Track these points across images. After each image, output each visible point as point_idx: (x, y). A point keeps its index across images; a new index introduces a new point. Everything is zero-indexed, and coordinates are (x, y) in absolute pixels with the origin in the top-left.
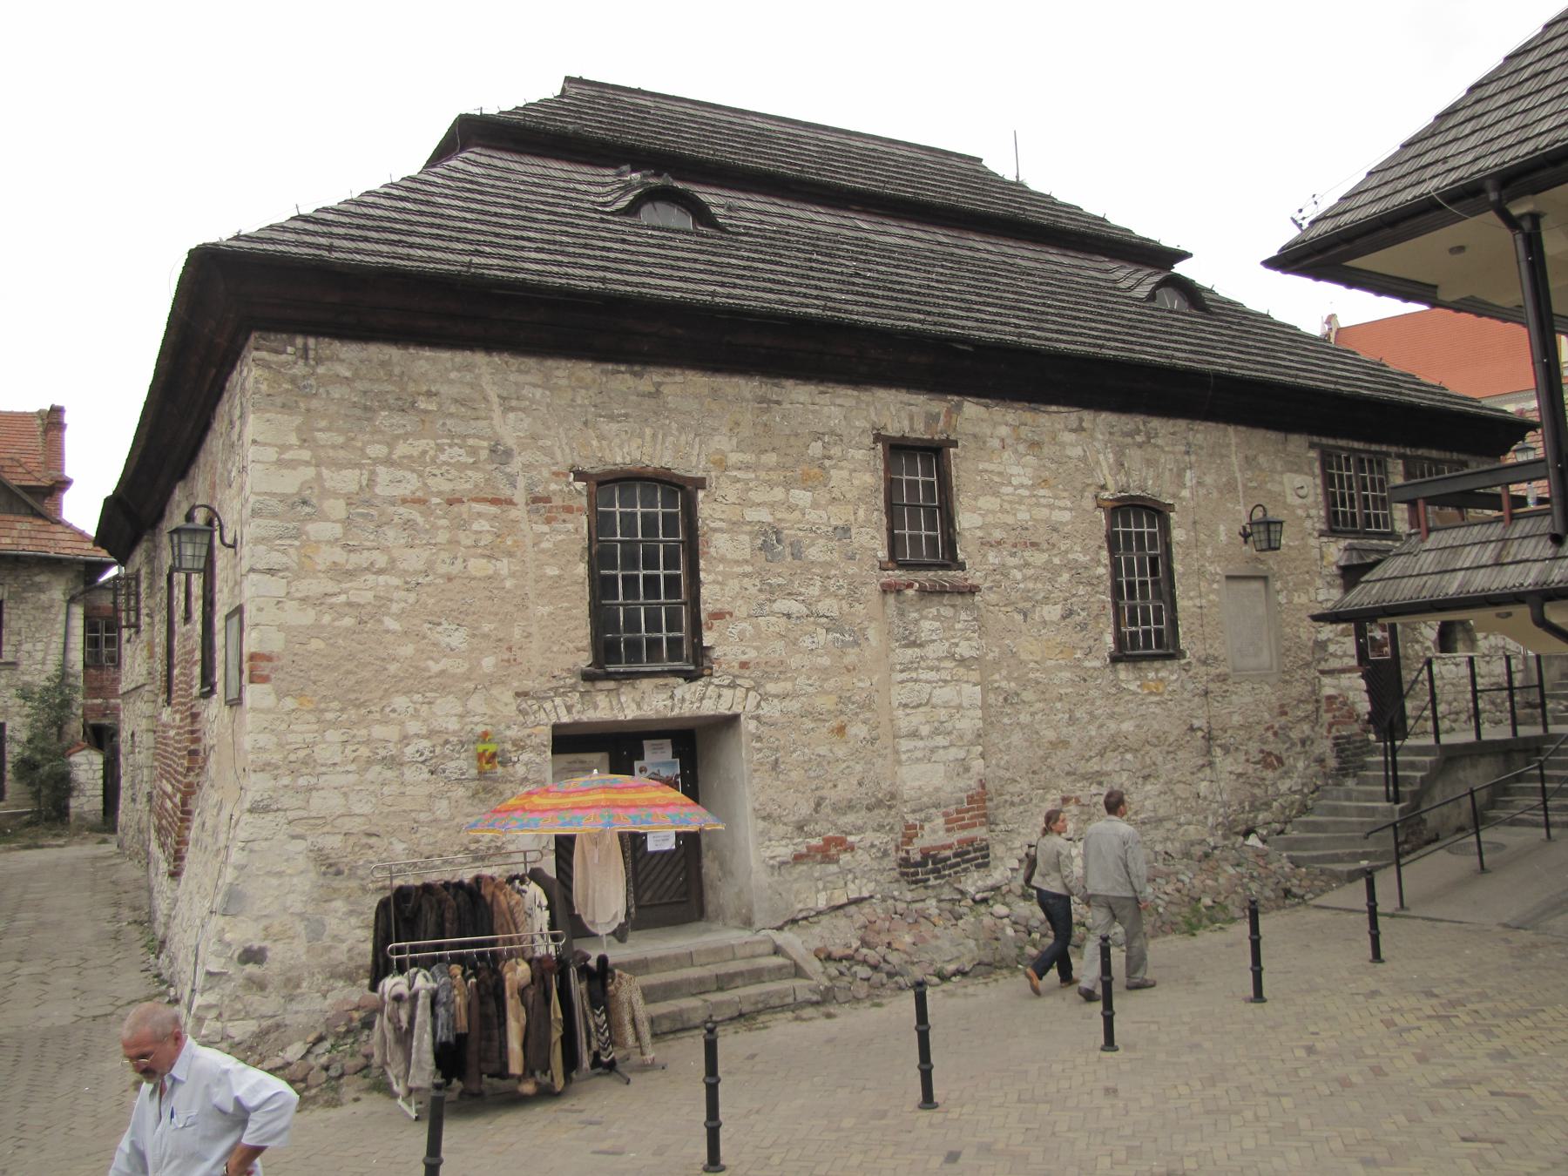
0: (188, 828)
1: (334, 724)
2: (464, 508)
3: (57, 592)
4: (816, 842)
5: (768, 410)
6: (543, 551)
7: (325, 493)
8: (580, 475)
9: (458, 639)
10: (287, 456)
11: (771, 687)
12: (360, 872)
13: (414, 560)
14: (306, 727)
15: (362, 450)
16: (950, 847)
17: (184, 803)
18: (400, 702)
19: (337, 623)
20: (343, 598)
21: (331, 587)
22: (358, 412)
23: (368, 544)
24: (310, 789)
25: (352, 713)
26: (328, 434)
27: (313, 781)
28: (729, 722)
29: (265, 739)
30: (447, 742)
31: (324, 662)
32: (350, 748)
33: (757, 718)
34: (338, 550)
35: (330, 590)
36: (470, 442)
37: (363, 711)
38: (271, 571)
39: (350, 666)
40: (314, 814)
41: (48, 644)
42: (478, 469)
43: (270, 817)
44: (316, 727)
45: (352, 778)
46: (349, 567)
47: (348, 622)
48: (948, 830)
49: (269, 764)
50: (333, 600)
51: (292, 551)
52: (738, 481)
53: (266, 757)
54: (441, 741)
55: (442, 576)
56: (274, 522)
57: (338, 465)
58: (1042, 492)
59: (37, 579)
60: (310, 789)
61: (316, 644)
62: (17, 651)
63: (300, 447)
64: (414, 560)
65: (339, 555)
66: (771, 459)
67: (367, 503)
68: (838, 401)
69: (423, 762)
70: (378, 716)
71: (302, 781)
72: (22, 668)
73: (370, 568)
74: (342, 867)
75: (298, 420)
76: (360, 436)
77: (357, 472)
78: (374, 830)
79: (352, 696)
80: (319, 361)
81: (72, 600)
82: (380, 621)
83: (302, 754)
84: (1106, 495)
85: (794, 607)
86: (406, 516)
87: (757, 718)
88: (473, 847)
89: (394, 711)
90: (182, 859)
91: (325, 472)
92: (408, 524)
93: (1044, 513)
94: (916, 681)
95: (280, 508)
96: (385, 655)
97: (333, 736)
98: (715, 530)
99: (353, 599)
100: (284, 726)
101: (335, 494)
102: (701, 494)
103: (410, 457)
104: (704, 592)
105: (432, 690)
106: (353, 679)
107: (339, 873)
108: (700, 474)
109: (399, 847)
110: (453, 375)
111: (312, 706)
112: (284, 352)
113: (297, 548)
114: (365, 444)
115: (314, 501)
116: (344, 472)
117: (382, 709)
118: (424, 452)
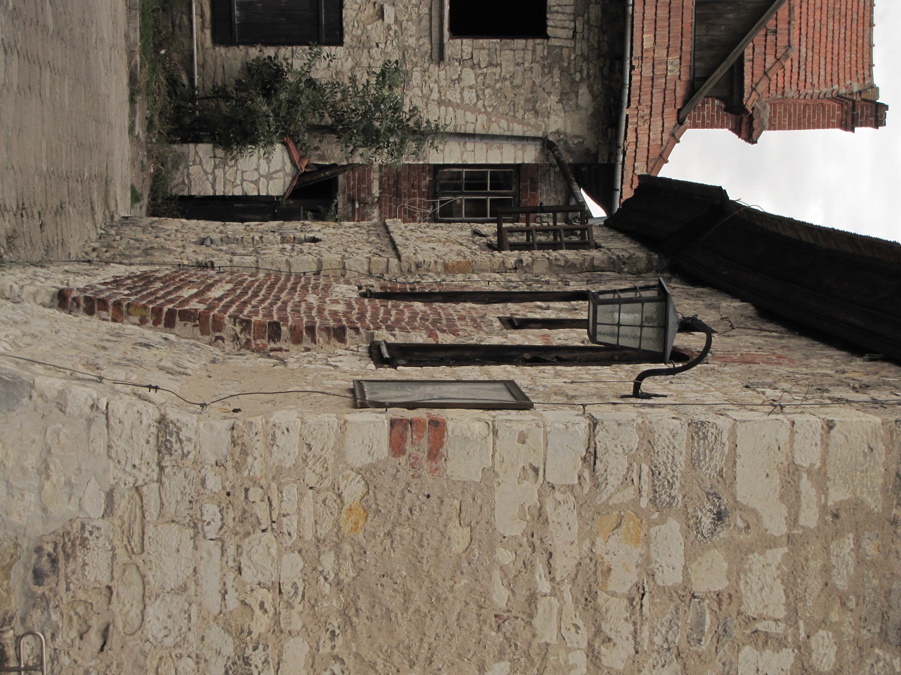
0: (143, 322)
1: (313, 569)
3: (563, 121)
7: (739, 555)
10: (805, 485)
12: (37, 615)
14: (309, 520)
15: (824, 623)
17: (187, 316)
19: (497, 574)
20: (544, 586)
21: (564, 564)
24: (196, 526)
25: (332, 603)
26: (850, 560)
27: (211, 531)
29: (289, 449)
31: (427, 552)
32: (268, 597)
34: (633, 577)
35: (559, 562)
37: (335, 622)
38: (592, 457)
39: (419, 599)
40: (150, 531)
41: (474, 109)
43: (151, 454)
44: (309, 536)
45: (213, 602)
46: (602, 597)
47: (500, 596)
49: (245, 453)
50: (541, 569)
51: (629, 493)
53: (258, 447)
56: (681, 460)
57: (792, 578)
59: (583, 90)
60: (196, 526)
61: (459, 536)
62: (461, 61)
63: (824, 508)
65: (623, 579)
67: (722, 633)
70: (325, 650)
71: (211, 511)
72: (434, 69)
73: (600, 637)
74: (50, 581)
75: (875, 503)
76: (848, 618)
77: (781, 613)
78: (114, 640)
79: (363, 604)
81: (547, 145)
82: (501, 655)
83: (261, 511)
90: (90, 311)
91: (778, 554)
95: (708, 472)
96: (437, 664)
97: (292, 568)
99: (542, 604)
101: (737, 572)
106: (395, 604)
107: (38, 576)
111: (346, 529)
113: (635, 502)
114: (836, 629)
115: (723, 534)
116: (779, 590)
117: (336, 658)
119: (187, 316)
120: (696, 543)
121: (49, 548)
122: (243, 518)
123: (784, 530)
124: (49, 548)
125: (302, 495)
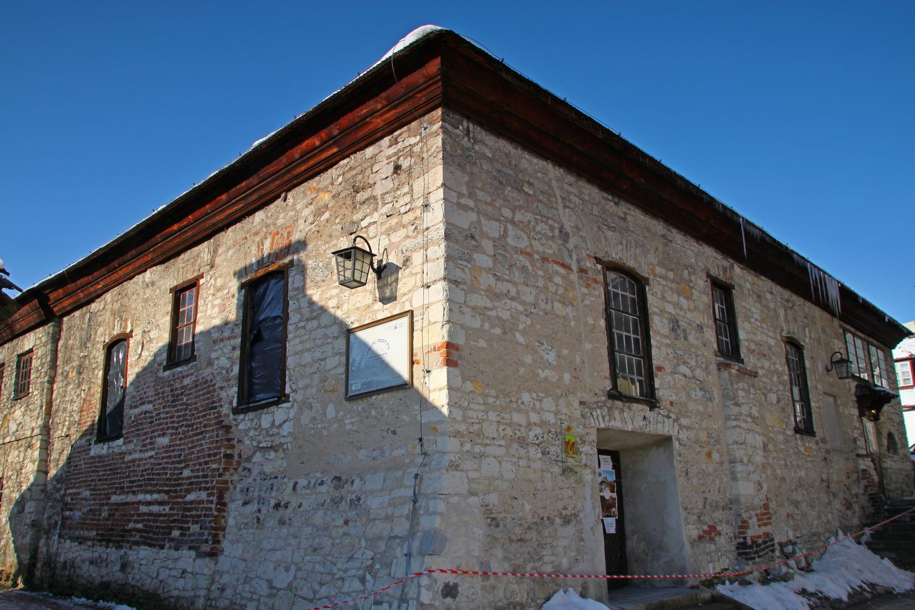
2: (550, 265)
4: (705, 528)
5: (666, 245)
6: (586, 306)
7: (484, 235)
8: (598, 260)
9: (551, 357)
10: (463, 201)
11: (684, 421)
13: (529, 295)
16: (759, 537)
17: (221, 497)
18: (526, 397)
19: (492, 331)
22: (496, 183)
23: (506, 277)
24: (482, 456)
27: (483, 449)
28: (665, 441)
30: (550, 432)
33: (678, 439)
36: (550, 222)
42: (554, 242)
44: (483, 408)
48: (759, 526)
49: (458, 432)
50: (489, 313)
51: (467, 270)
52: (660, 284)
54: (547, 430)
55: (542, 310)
56: (457, 247)
58: (764, 326)
60: (482, 456)
61: (482, 343)
64: (529, 295)
65: (492, 281)
66: (671, 275)
68: (692, 248)
69: (538, 445)
71: (477, 449)
73: (507, 295)
80: (476, 141)
83: (477, 427)
84: (784, 334)
85: (688, 372)
86: (522, 263)
87: (678, 439)
88: (564, 512)
89: (523, 403)
90: (219, 542)
91: (483, 221)
92: (524, 269)
93: (765, 338)
94: (740, 427)
98: (655, 313)
100: (465, 404)
102: (647, 288)
103: (523, 222)
104: (654, 352)
105: (541, 392)
108: (646, 275)
109: (527, 507)
110: (539, 175)
112: (458, 128)
115: (477, 237)
118: (529, 222)
119: (221, 497)
120: (478, 248)
121: (489, 520)
122: (478, 435)
123: (475, 214)
124: (489, 520)
125: (472, 409)
